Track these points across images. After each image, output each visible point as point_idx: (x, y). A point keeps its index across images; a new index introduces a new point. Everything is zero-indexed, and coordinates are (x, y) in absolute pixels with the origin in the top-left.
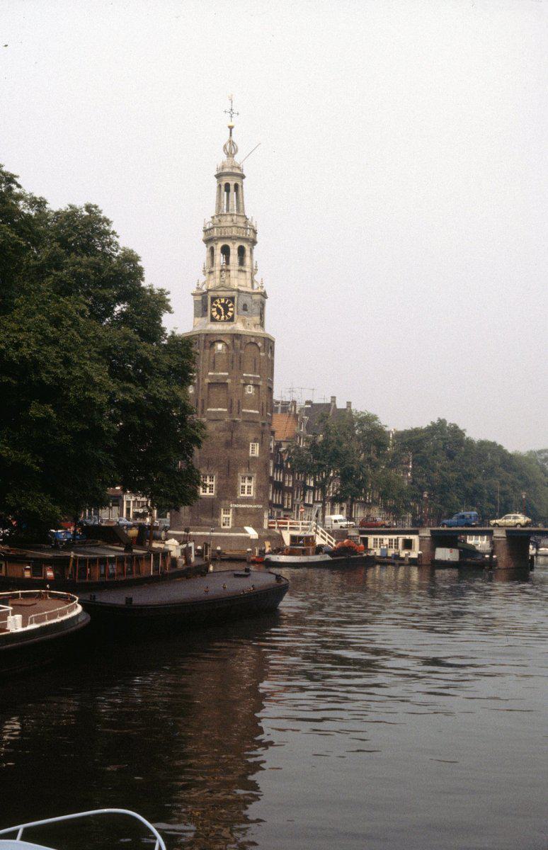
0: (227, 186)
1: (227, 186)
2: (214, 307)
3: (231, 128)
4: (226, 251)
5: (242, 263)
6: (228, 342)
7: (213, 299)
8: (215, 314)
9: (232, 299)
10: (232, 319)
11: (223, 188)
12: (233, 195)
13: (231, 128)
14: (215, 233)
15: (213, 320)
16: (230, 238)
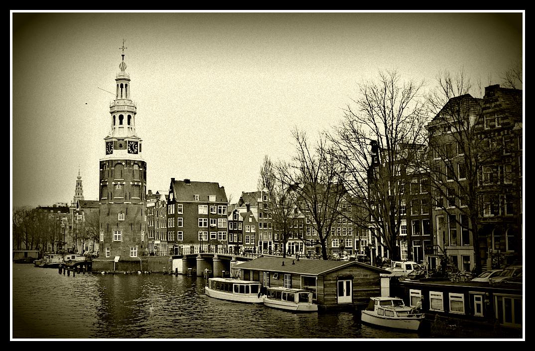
0: (126, 85)
1: (126, 85)
2: (129, 146)
3: (123, 56)
4: (129, 117)
5: (129, 123)
6: (140, 165)
7: (129, 142)
8: (130, 149)
9: (137, 143)
10: (137, 153)
11: (124, 86)
12: (124, 89)
13: (123, 56)
14: (116, 109)
15: (129, 152)
16: (132, 112)
